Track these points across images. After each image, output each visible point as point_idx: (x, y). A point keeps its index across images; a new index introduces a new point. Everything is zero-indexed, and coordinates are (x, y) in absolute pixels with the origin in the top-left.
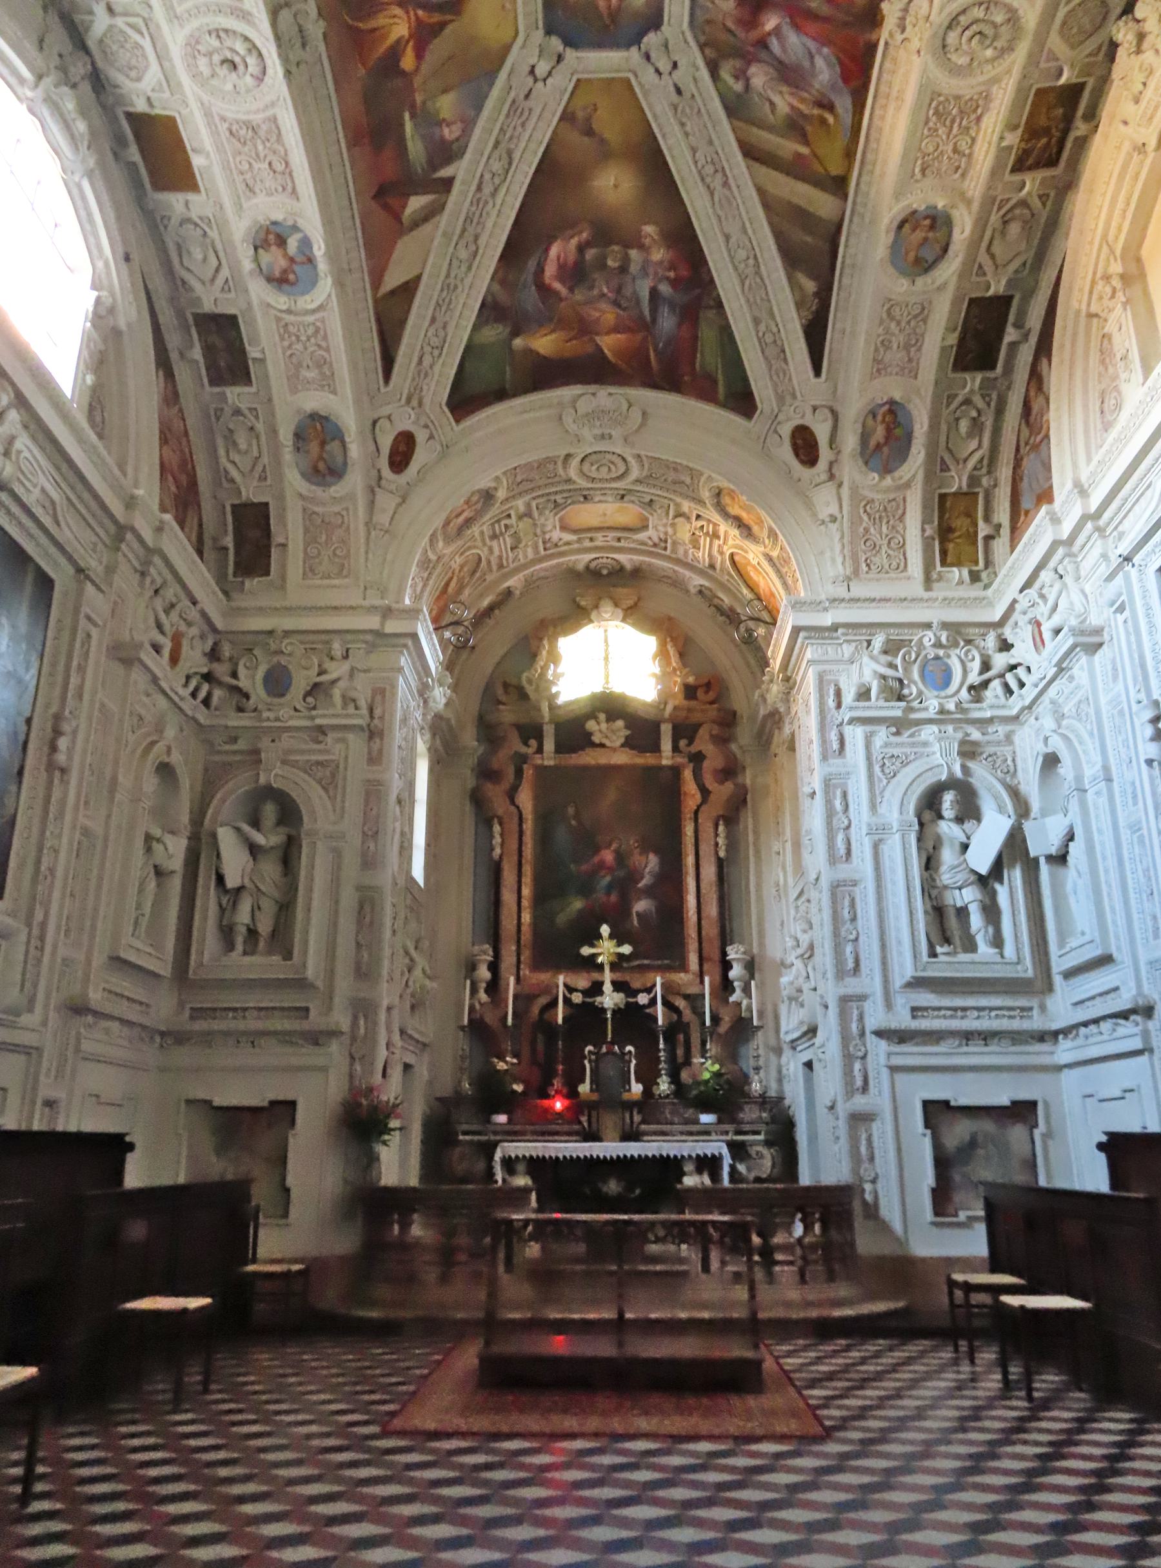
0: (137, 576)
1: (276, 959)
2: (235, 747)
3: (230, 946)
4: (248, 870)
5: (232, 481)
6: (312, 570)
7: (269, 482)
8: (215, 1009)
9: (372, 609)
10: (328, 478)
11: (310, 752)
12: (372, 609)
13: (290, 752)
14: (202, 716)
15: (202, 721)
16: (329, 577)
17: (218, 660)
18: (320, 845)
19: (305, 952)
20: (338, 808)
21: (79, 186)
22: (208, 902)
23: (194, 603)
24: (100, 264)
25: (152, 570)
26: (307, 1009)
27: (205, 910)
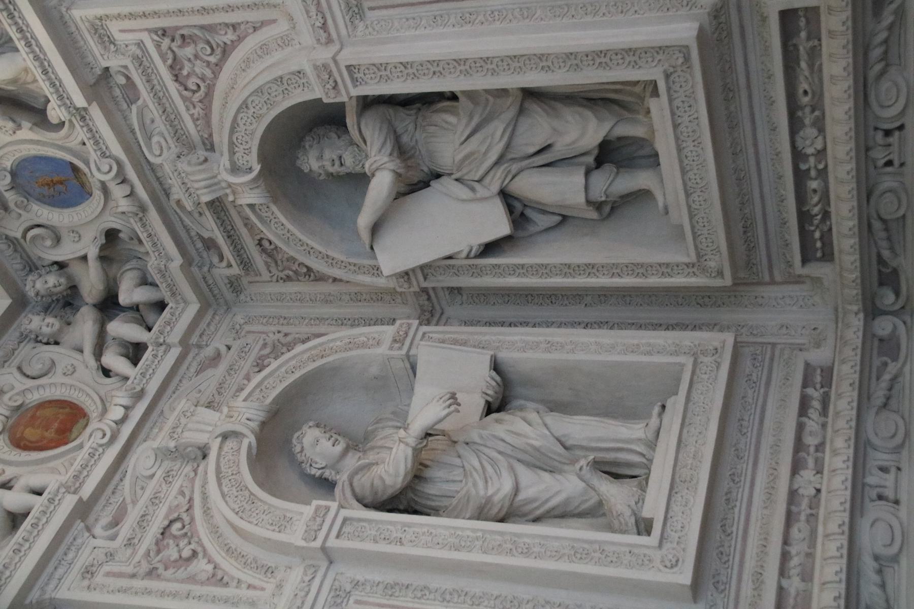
1: (659, 108)
2: (221, 241)
3: (642, 196)
4: (461, 191)
8: (803, 217)
11: (160, 98)
13: (179, 135)
15: (193, 308)
17: (74, 289)
18: (348, 56)
19: (632, 54)
20: (254, 16)
26: (788, 17)
27: (569, 269)
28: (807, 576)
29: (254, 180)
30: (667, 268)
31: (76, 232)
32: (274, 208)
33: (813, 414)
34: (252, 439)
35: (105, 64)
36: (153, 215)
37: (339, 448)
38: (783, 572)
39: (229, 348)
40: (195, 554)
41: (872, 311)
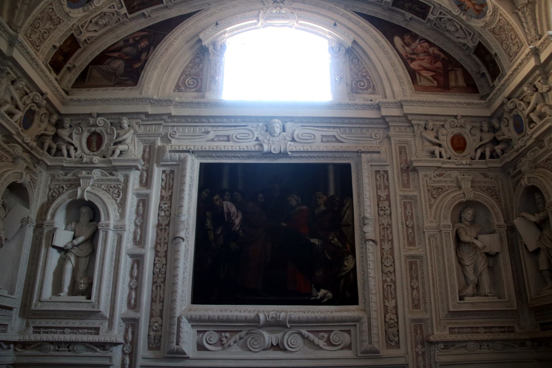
0: (411, 128)
5: (465, 45)
6: (510, 56)
7: (472, 34)
9: (527, 58)
10: (484, 9)
12: (527, 58)
14: (496, 164)
16: (517, 52)
21: (301, 24)
22: (527, 263)
23: (456, 117)
24: (328, 36)
25: (413, 122)
28: (459, 333)
29: (526, 185)
30: (530, 292)
31: (509, 131)
32: (523, 189)
33: (500, 330)
34: (465, 201)
35: (545, 140)
36: (516, 154)
37: (469, 220)
38: (458, 328)
39: (491, 178)
40: (435, 198)
41: (532, 340)
